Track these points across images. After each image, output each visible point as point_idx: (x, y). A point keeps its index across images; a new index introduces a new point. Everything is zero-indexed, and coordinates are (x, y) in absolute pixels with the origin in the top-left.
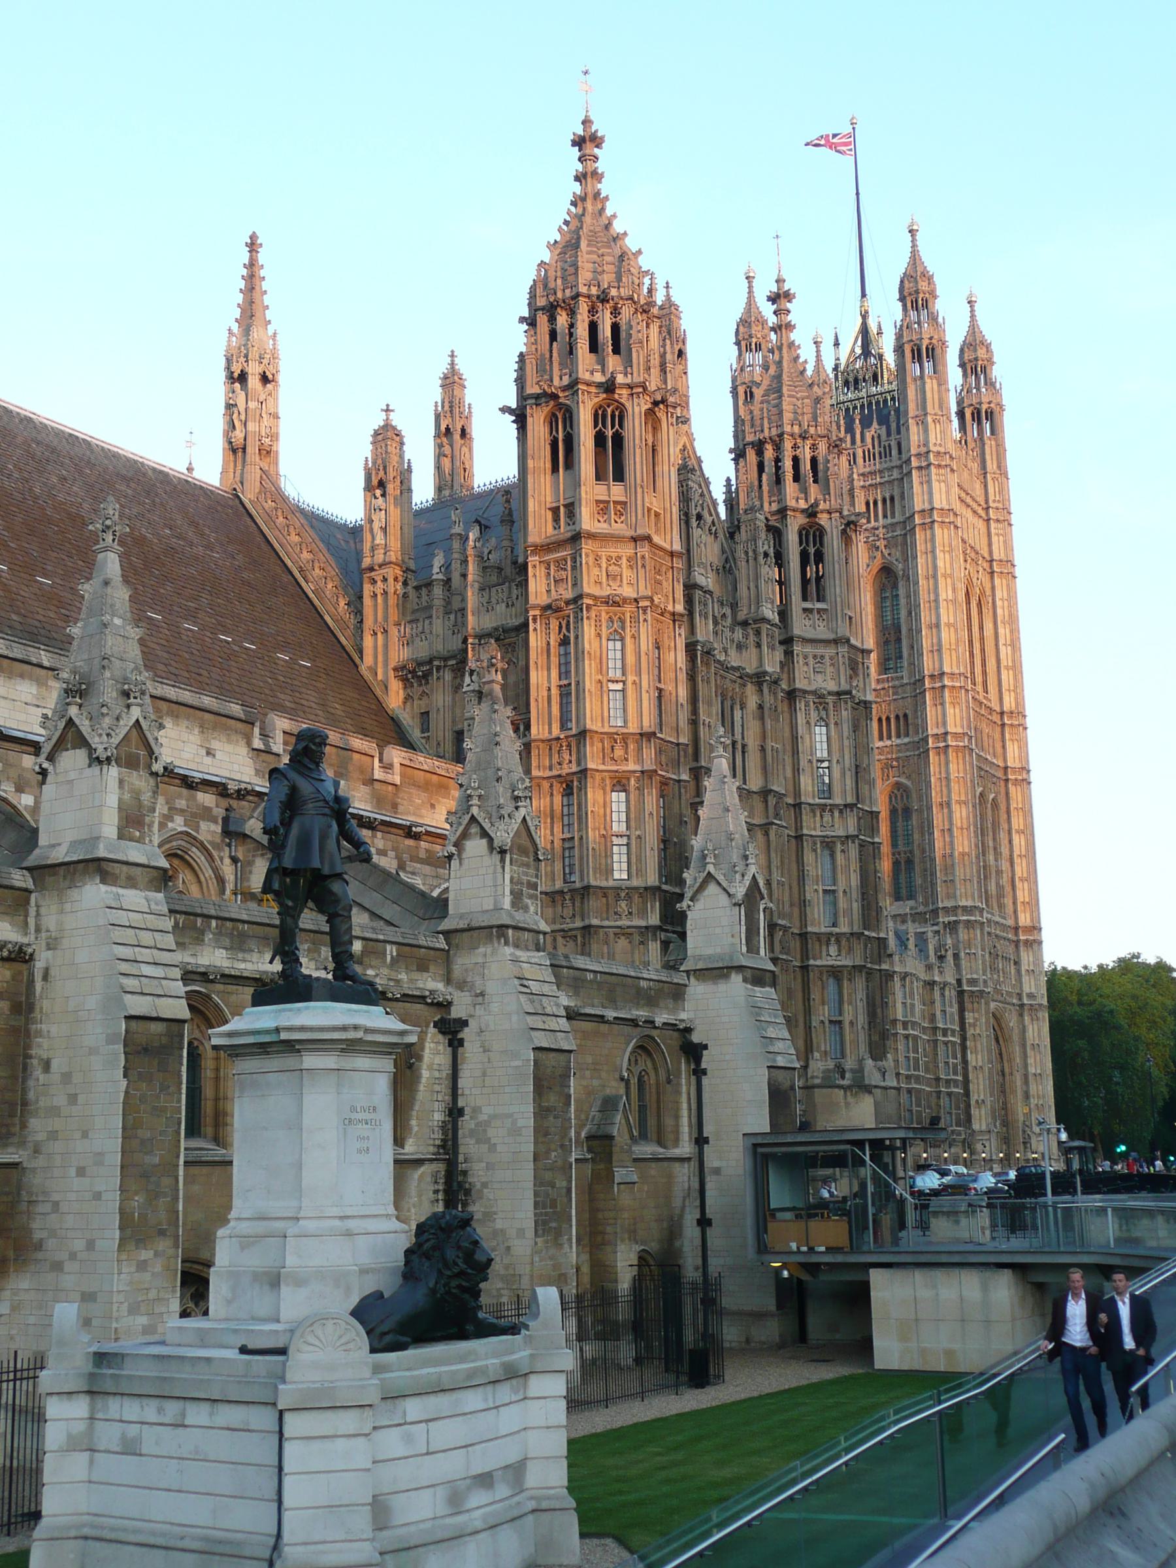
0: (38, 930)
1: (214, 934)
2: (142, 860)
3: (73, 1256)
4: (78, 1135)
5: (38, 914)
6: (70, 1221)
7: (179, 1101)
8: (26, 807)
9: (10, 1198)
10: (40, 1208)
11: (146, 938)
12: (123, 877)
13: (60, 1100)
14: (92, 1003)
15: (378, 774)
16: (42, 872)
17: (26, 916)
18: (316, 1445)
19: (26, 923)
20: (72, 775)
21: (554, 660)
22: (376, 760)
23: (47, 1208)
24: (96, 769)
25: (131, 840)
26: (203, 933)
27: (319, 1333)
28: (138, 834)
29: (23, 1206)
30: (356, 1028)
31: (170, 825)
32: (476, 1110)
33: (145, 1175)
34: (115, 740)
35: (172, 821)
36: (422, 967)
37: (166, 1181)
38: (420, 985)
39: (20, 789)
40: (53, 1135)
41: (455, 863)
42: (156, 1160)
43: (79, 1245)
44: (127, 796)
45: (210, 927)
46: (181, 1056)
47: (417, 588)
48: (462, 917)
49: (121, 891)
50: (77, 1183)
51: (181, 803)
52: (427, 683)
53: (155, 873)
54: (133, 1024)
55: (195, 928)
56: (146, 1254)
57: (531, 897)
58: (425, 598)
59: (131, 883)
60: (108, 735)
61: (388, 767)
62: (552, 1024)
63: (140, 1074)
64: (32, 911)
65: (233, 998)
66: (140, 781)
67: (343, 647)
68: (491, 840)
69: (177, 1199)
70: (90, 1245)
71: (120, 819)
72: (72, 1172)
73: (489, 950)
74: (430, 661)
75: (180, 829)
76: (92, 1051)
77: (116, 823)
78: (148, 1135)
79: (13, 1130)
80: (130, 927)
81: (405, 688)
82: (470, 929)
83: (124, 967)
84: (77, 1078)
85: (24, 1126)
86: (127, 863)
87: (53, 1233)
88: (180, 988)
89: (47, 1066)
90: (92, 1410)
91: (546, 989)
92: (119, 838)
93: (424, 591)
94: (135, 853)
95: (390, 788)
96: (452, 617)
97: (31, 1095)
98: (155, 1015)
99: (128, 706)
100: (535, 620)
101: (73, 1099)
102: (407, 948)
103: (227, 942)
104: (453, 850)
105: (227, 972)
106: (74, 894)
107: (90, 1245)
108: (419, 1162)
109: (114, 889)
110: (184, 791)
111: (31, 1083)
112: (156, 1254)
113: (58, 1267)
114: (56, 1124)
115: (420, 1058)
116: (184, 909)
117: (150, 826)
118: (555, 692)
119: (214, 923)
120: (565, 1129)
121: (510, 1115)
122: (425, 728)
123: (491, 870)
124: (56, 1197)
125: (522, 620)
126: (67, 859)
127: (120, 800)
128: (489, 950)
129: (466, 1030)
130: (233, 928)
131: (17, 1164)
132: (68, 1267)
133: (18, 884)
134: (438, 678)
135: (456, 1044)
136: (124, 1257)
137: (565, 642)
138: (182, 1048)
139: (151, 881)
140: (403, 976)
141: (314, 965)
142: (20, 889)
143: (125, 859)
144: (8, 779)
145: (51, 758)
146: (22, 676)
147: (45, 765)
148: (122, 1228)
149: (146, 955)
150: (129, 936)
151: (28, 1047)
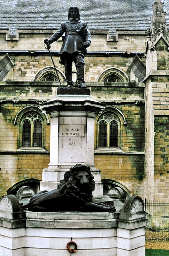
17: (144, 94)
19: (144, 96)
25: (162, 69)
28: (164, 67)
34: (155, 44)
44: (160, 58)
49: (157, 83)
59: (162, 81)
60: (153, 43)
71: (158, 64)
77: (156, 65)
80: (159, 92)
83: (156, 103)
92: (157, 69)
94: (162, 73)
99: (159, 34)
109: (155, 83)
127: (158, 59)
133: (140, 86)
145: (146, 53)
147: (146, 55)
150: (159, 95)
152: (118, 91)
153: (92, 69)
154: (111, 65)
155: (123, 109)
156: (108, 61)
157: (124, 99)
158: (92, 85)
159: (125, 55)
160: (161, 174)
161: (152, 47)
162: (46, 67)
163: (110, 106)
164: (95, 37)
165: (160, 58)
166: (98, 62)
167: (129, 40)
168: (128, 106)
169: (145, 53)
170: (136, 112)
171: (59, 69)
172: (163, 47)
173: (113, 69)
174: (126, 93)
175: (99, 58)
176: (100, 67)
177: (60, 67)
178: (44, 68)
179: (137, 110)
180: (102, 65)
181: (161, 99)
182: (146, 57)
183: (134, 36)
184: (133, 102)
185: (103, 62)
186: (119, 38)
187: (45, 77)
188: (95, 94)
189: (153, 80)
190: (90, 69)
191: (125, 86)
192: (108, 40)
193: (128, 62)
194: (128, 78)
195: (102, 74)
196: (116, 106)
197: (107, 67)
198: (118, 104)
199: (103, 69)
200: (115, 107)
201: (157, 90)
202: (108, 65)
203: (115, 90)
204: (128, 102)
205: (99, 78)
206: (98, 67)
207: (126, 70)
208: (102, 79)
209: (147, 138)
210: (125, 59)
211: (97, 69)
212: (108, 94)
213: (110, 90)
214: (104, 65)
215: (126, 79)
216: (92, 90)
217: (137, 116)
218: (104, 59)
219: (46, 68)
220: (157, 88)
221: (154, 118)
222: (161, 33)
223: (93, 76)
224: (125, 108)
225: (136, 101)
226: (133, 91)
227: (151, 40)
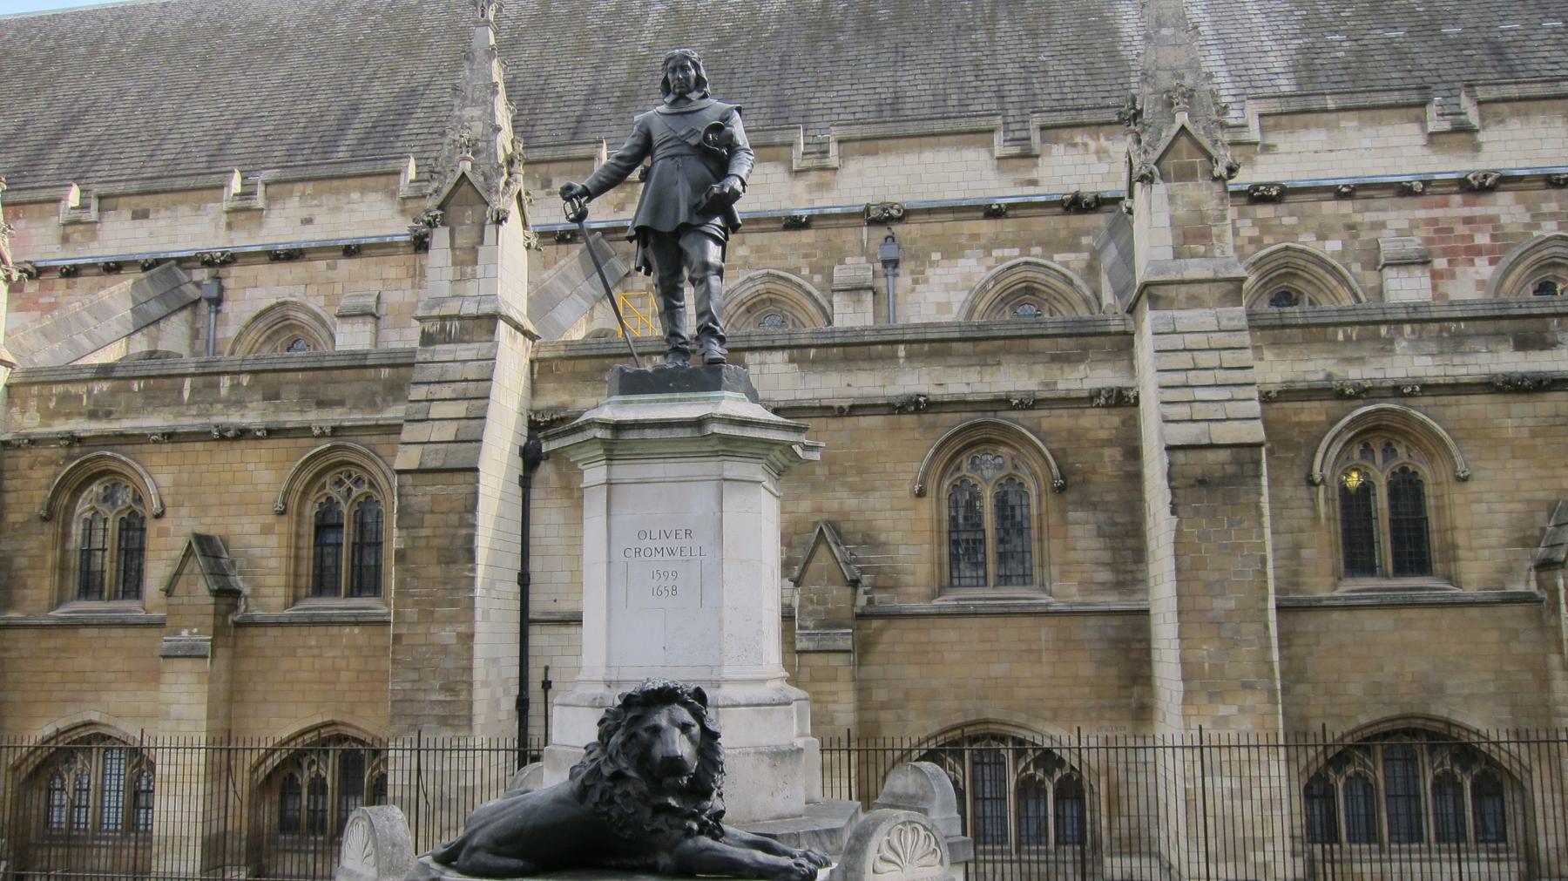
1: (1409, 341)
2: (1210, 275)
7: (1261, 536)
8: (1333, 254)
9: (1144, 645)
12: (1182, 297)
17: (1131, 359)
19: (1132, 367)
26: (1391, 341)
28: (1202, 249)
31: (1536, 233)
33: (1216, 623)
34: (1155, 155)
35: (1538, 227)
37: (1250, 630)
39: (1322, 237)
42: (1231, 604)
45: (1402, 334)
46: (1259, 485)
49: (1177, 314)
51: (1547, 207)
53: (1230, 286)
54: (1180, 457)
55: (1378, 338)
56: (1222, 710)
59: (1195, 302)
65: (1453, 411)
66: (1201, 193)
69: (1269, 648)
71: (1174, 237)
78: (1216, 576)
79: (1140, 576)
80: (1185, 350)
86: (1183, 282)
88: (1255, 407)
94: (1195, 269)
98: (1207, 441)
103: (1433, 347)
105: (1430, 381)
109: (1169, 313)
110: (1554, 192)
112: (1242, 710)
117: (1220, 237)
119: (1407, 328)
127: (1172, 218)
130: (1441, 331)
133: (1113, 329)
136: (1193, 710)
138: (1259, 476)
139: (1224, 296)
142: (1117, 333)
143: (1179, 277)
144: (1306, 230)
145: (1131, 196)
146: (1306, 126)
148: (1185, 679)
149: (1207, 378)
150: (1183, 360)
152: (1019, 353)
153: (939, 271)
154: (1016, 252)
155: (1046, 425)
156: (1002, 237)
158: (907, 337)
159: (1076, 205)
161: (1144, 171)
162: (753, 274)
163: (990, 417)
164: (945, 145)
165: (1181, 212)
166: (963, 240)
167: (1085, 145)
168: (1064, 412)
169: (1126, 195)
170: (1103, 434)
171: (803, 278)
172: (1193, 167)
173: (1027, 263)
174: (1055, 359)
175: (966, 224)
176: (972, 262)
177: (805, 272)
178: (742, 279)
180: (980, 252)
181: (1193, 377)
182: (1130, 211)
183: (1107, 128)
184: (1085, 394)
185: (983, 241)
186: (1043, 140)
187: (748, 311)
188: (925, 370)
189: (1155, 302)
190: (929, 272)
191: (1050, 331)
192: (997, 154)
193: (1087, 233)
194: (1093, 299)
195: (983, 287)
196: (1014, 414)
197: (1004, 259)
199: (984, 269)
200: (1005, 417)
201: (1177, 341)
202: (1007, 252)
203: (1008, 352)
204: (1063, 394)
205: (967, 305)
206: (961, 262)
207: (1083, 265)
208: (981, 306)
209: (1152, 545)
210: (1077, 221)
211: (958, 270)
213: (985, 353)
214: (988, 251)
215: (1086, 301)
216: (909, 357)
217: (1107, 452)
218: (987, 227)
219: (751, 279)
220: (1174, 332)
221: (1166, 460)
222: (1181, 110)
223: (943, 298)
225: (1098, 393)
226: (1085, 349)
227: (1139, 142)
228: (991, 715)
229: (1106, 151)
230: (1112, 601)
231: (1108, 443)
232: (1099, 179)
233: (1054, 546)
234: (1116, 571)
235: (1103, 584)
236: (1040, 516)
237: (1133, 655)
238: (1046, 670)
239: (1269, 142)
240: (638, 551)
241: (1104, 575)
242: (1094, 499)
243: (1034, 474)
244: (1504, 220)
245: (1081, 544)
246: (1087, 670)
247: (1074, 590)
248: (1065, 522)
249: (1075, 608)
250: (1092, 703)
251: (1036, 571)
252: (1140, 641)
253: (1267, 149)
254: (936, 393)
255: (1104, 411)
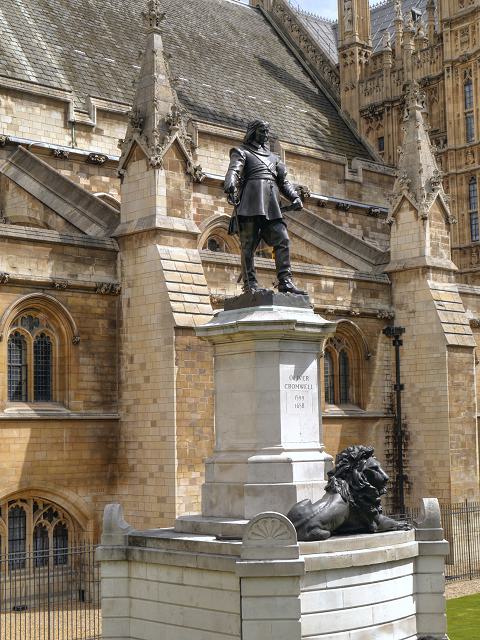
0: (122, 275)
2: (184, 229)
3: (152, 475)
4: (151, 401)
5: (122, 265)
6: (149, 454)
10: (132, 446)
11: (187, 277)
13: (140, 380)
14: (155, 319)
15: (348, 176)
16: (122, 239)
17: (116, 267)
18: (263, 601)
19: (116, 272)
20: (138, 177)
21: (460, 95)
22: (347, 168)
23: (136, 446)
24: (151, 171)
27: (262, 527)
29: (122, 445)
30: (289, 322)
31: (216, 212)
32: (412, 386)
33: (193, 426)
35: (217, 210)
36: (374, 295)
38: (373, 306)
40: (137, 402)
41: (393, 228)
42: (199, 417)
43: (154, 469)
44: (172, 188)
47: (374, 58)
48: (399, 262)
49: (170, 249)
50: (152, 431)
52: (382, 119)
56: (195, 475)
57: (445, 248)
58: (379, 64)
61: (354, 172)
62: (460, 329)
63: (186, 363)
64: (119, 265)
67: (328, 99)
68: (416, 211)
70: (161, 469)
71: (168, 203)
72: (149, 424)
73: (417, 283)
74: (383, 105)
75: (222, 215)
76: (157, 350)
77: (165, 205)
78: (193, 401)
79: (114, 399)
81: (367, 123)
82: (405, 270)
84: (148, 366)
85: (120, 397)
87: (140, 462)
89: (131, 360)
90: (129, 571)
91: (456, 307)
93: (378, 60)
94: (178, 224)
95: (356, 185)
96: (396, 74)
97: (123, 377)
100: (448, 70)
101: (147, 379)
102: (363, 283)
104: (392, 219)
106: (142, 252)
107: (161, 469)
108: (376, 419)
111: (123, 370)
113: (143, 481)
114: (139, 395)
115: (374, 353)
116: (216, 260)
118: (462, 116)
120: (471, 398)
121: (432, 389)
122: (381, 148)
123: (417, 231)
124: (140, 439)
125: (440, 72)
126: (137, 230)
128: (417, 283)
129: (404, 334)
131: (117, 420)
132: (149, 481)
133: (108, 247)
134: (388, 115)
135: (398, 343)
137: (468, 83)
140: (361, 301)
141: (265, 283)
145: (125, 167)
151: (120, 347)
155: (71, 301)
157: (72, 276)
160: (191, 468)
170: (99, 311)
174: (78, 261)
179: (101, 305)
188: (5, 257)
191: (76, 243)
196: (53, 293)
198: (62, 288)
204: (82, 284)
212: (36, 260)
224: (76, 299)
228: (35, 485)
229: (11, 109)
230: (99, 413)
231: (101, 316)
232: (5, 126)
233: (72, 379)
234: (102, 395)
235: (95, 402)
236: (62, 359)
237: (110, 446)
238: (66, 455)
239: (100, 127)
240: (290, 386)
241: (95, 398)
242: (94, 350)
243: (59, 330)
244: (203, 202)
245: (85, 378)
246: (86, 455)
247: (81, 406)
248: (78, 364)
249: (84, 417)
250: (88, 475)
251: (57, 394)
252: (113, 437)
253: (99, 132)
254: (13, 274)
255: (99, 296)
